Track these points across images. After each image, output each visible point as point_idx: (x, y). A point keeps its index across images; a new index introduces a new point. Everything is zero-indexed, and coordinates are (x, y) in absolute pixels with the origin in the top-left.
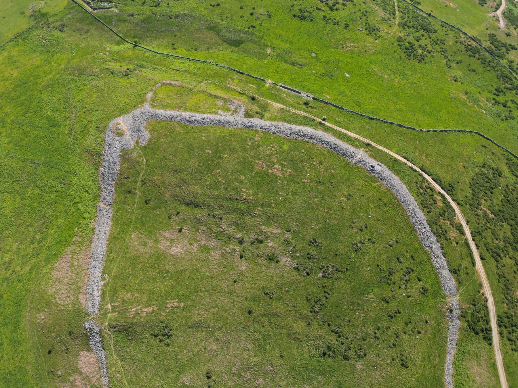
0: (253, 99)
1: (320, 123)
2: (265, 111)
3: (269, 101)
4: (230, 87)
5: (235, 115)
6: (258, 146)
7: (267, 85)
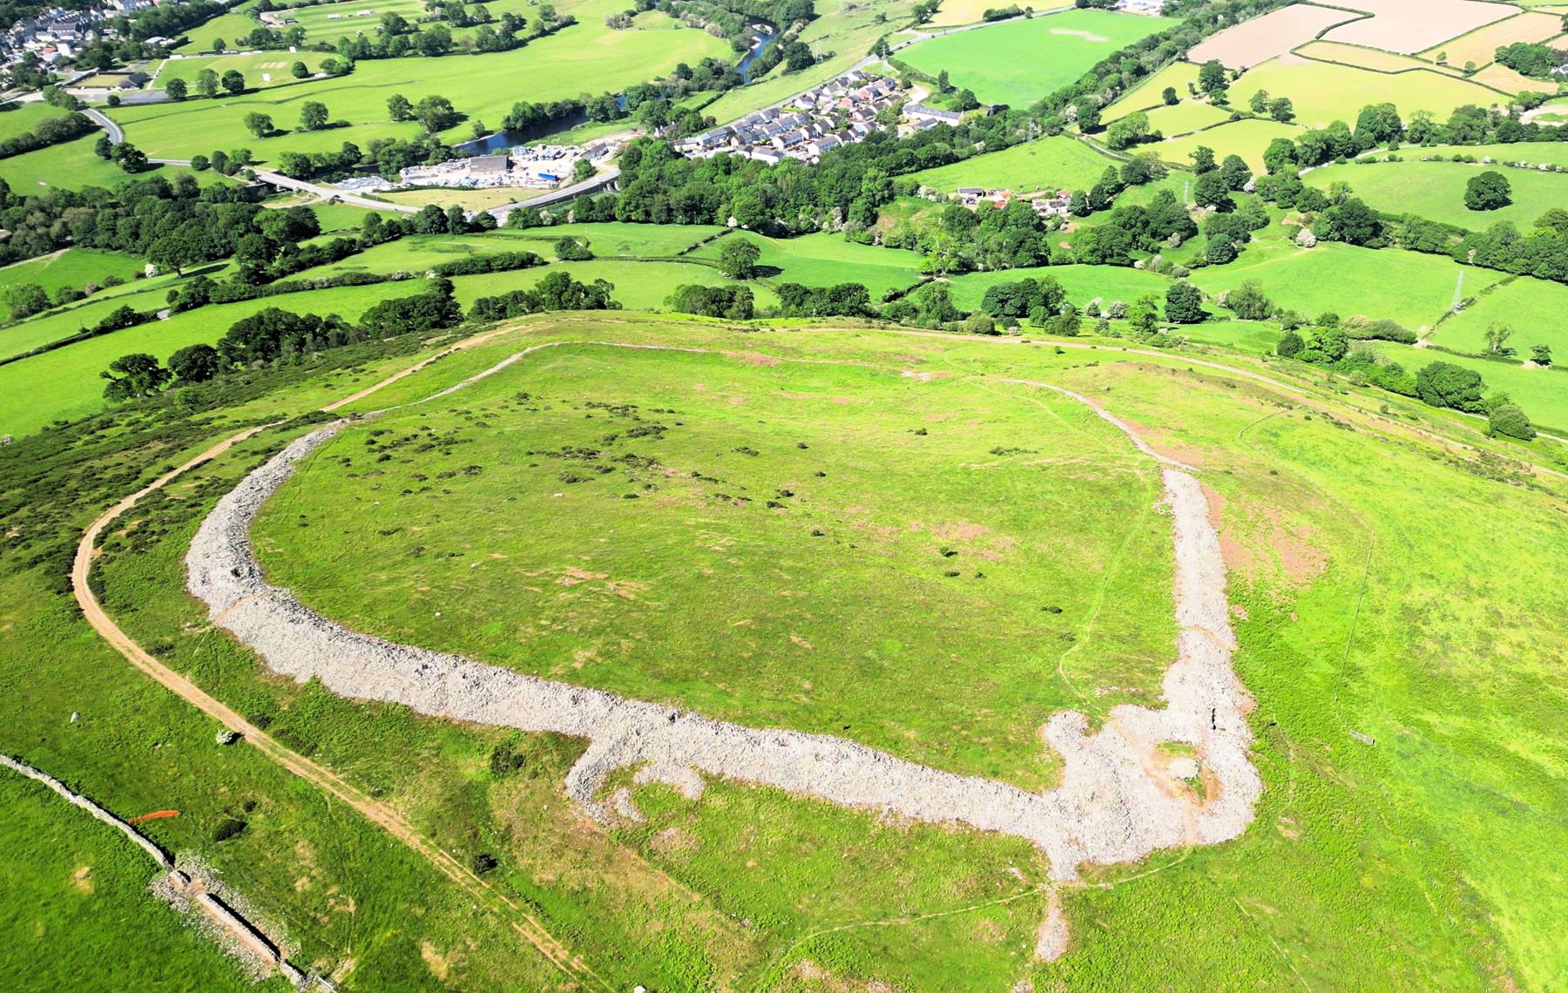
5: (627, 758)
6: (598, 632)
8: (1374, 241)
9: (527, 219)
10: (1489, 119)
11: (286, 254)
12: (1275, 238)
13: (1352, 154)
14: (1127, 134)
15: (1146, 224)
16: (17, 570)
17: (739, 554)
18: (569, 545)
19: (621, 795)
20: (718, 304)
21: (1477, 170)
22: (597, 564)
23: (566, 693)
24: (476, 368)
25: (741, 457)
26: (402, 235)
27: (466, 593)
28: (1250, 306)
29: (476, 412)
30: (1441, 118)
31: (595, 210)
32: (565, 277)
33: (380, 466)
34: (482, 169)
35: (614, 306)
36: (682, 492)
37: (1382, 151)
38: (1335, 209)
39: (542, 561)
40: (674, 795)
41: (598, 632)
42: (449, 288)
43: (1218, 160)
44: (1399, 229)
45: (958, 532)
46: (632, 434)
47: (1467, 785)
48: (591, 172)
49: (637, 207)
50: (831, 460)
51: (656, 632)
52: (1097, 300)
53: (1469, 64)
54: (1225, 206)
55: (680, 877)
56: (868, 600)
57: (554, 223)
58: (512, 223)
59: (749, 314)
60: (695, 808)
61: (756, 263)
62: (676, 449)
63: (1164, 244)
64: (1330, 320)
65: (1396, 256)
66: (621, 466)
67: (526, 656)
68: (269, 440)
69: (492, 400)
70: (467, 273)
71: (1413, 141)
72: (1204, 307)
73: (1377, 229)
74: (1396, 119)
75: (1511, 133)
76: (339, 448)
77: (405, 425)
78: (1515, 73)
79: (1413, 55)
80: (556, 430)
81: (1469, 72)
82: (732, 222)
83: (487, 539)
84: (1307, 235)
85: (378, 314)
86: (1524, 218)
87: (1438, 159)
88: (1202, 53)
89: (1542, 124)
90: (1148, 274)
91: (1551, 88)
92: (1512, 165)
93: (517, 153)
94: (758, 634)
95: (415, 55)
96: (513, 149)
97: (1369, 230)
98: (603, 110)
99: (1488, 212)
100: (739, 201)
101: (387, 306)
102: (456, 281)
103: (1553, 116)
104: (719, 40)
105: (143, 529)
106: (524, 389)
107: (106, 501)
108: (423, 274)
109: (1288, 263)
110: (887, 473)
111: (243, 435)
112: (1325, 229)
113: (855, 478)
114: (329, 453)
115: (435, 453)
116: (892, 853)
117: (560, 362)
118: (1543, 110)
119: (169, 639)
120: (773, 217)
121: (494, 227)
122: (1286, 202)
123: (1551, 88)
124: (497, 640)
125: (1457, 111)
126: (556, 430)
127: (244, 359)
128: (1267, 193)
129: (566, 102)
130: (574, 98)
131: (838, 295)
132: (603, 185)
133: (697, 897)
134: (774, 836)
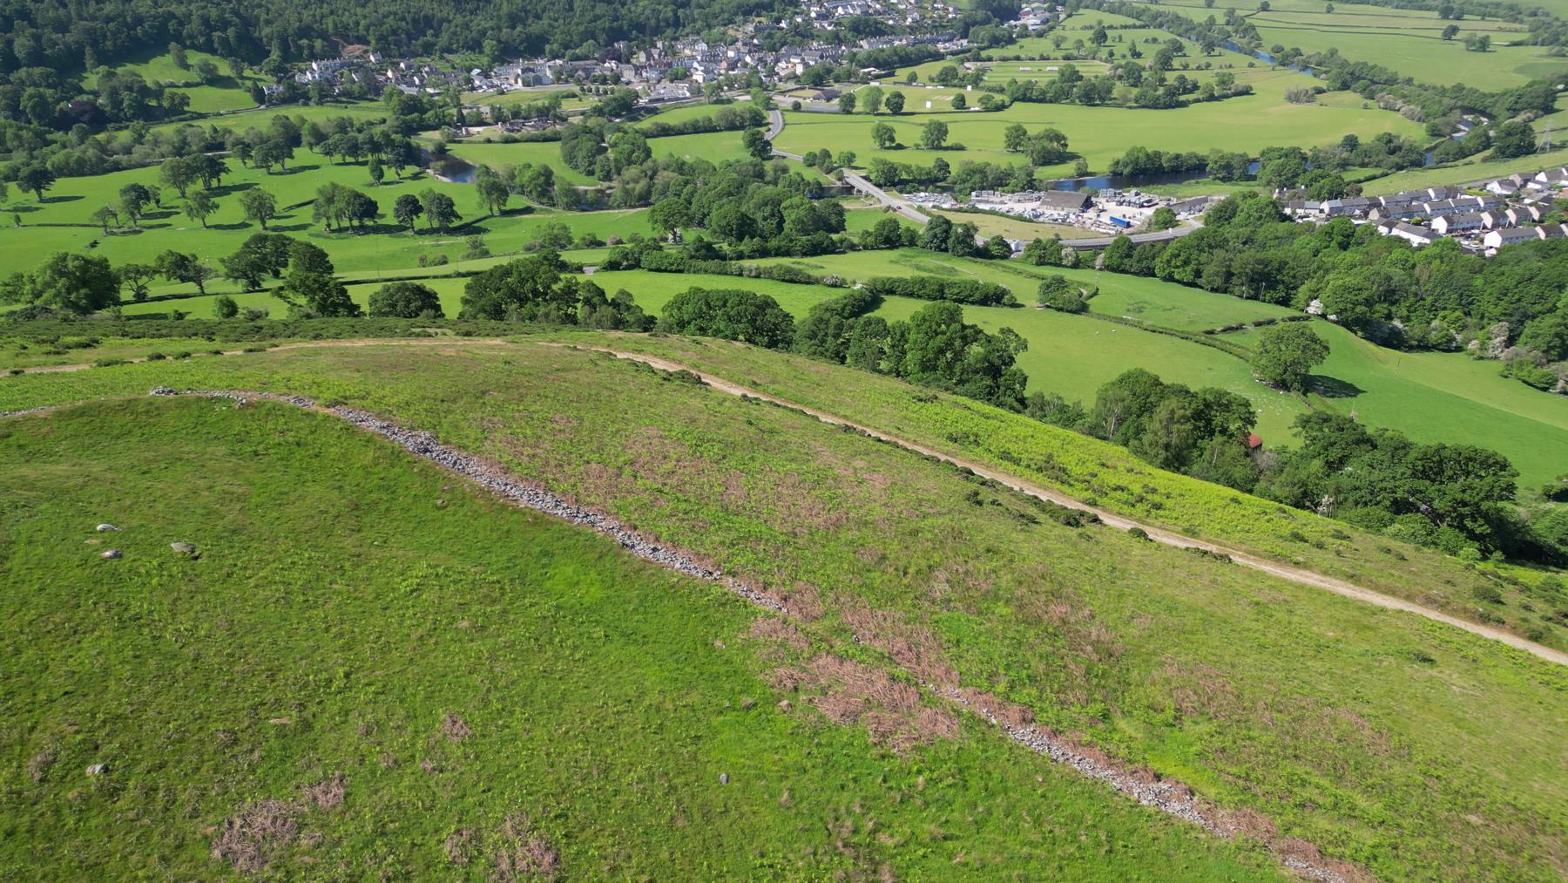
49: (1186, 263)
57: (1076, 265)
61: (1314, 371)
70: (911, 295)
82: (1315, 307)
95: (1073, 102)
100: (1334, 281)
104: (1414, 124)
120: (1389, 317)
121: (1004, 257)
130: (1202, 151)
131: (1435, 466)
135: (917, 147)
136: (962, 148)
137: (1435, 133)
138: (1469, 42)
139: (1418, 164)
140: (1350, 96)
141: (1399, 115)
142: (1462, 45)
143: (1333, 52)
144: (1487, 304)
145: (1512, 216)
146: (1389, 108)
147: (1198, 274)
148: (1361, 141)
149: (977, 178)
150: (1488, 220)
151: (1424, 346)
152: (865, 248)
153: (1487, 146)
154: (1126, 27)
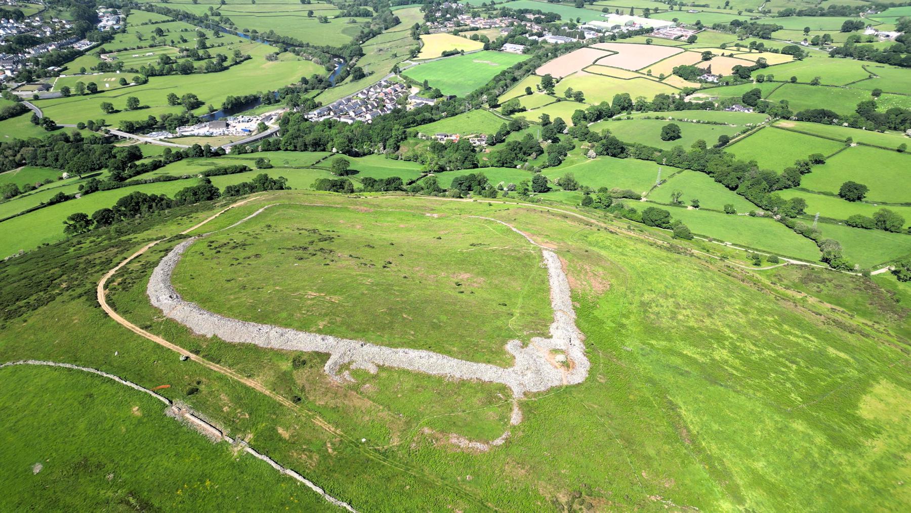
0: (297, 400)
1: (197, 352)
2: (285, 373)
3: (268, 392)
4: (336, 428)
5: (347, 360)
7: (250, 436)
8: (621, 155)
9: (240, 150)
10: (671, 100)
11: (131, 167)
12: (577, 154)
13: (611, 116)
14: (511, 108)
15: (521, 149)
16: (73, 299)
17: (377, 285)
18: (306, 283)
19: (346, 373)
20: (337, 186)
21: (666, 122)
22: (319, 290)
23: (319, 337)
24: (245, 215)
25: (367, 248)
26: (182, 158)
27: (268, 302)
28: (569, 184)
29: (251, 233)
30: (650, 99)
31: (271, 146)
32: (266, 175)
33: (217, 255)
34: (215, 127)
35: (289, 188)
36: (347, 263)
37: (624, 115)
38: (604, 141)
39: (297, 289)
40: (367, 372)
41: (326, 315)
42: (209, 182)
43: (552, 120)
44: (632, 150)
45: (464, 276)
46: (320, 240)
47: (668, 365)
48: (266, 128)
50: (405, 249)
51: (349, 315)
52: (502, 183)
53: (662, 75)
54: (555, 140)
55: (374, 401)
56: (431, 302)
57: (252, 152)
58: (233, 152)
59: (352, 191)
60: (375, 377)
62: (340, 246)
63: (529, 158)
64: (604, 190)
65: (632, 161)
66: (319, 253)
67: (299, 324)
68: (167, 245)
69: (257, 228)
71: (637, 110)
72: (549, 185)
73: (623, 150)
74: (630, 100)
75: (680, 106)
76: (196, 248)
77: (222, 239)
78: (682, 79)
79: (636, 71)
80: (288, 239)
81: (662, 78)
83: (272, 282)
84: (592, 153)
85: (183, 193)
86: (686, 144)
87: (649, 118)
88: (542, 71)
89: (694, 102)
90: (523, 172)
91: (697, 85)
92: (681, 120)
93: (230, 120)
94: (390, 314)
96: (228, 118)
97: (619, 150)
98: (268, 99)
99: (671, 141)
101: (187, 190)
102: (212, 178)
103: (699, 98)
105: (124, 282)
106: (269, 223)
107: (103, 271)
108: (196, 176)
109: (583, 164)
110: (429, 254)
111: (152, 244)
112: (600, 150)
113: (415, 256)
114: (193, 250)
115: (239, 249)
116: (453, 391)
117: (281, 211)
118: (694, 95)
119: (149, 323)
122: (582, 138)
123: (697, 85)
124: (285, 319)
125: (656, 96)
126: (288, 239)
127: (125, 215)
128: (573, 133)
129: (251, 96)
130: (254, 93)
132: (272, 134)
133: (381, 407)
134: (407, 386)
135: (126, 110)
136: (148, 107)
137: (329, 70)
138: (320, 18)
139: (330, 86)
140: (289, 55)
141: (312, 62)
142: (317, 20)
143: (272, 32)
144: (375, 138)
145: (370, 107)
146: (307, 59)
147: (295, 147)
148: (307, 78)
149: (176, 122)
150: (364, 110)
151: (365, 155)
152: (171, 162)
153: (349, 75)
154: (164, 22)
